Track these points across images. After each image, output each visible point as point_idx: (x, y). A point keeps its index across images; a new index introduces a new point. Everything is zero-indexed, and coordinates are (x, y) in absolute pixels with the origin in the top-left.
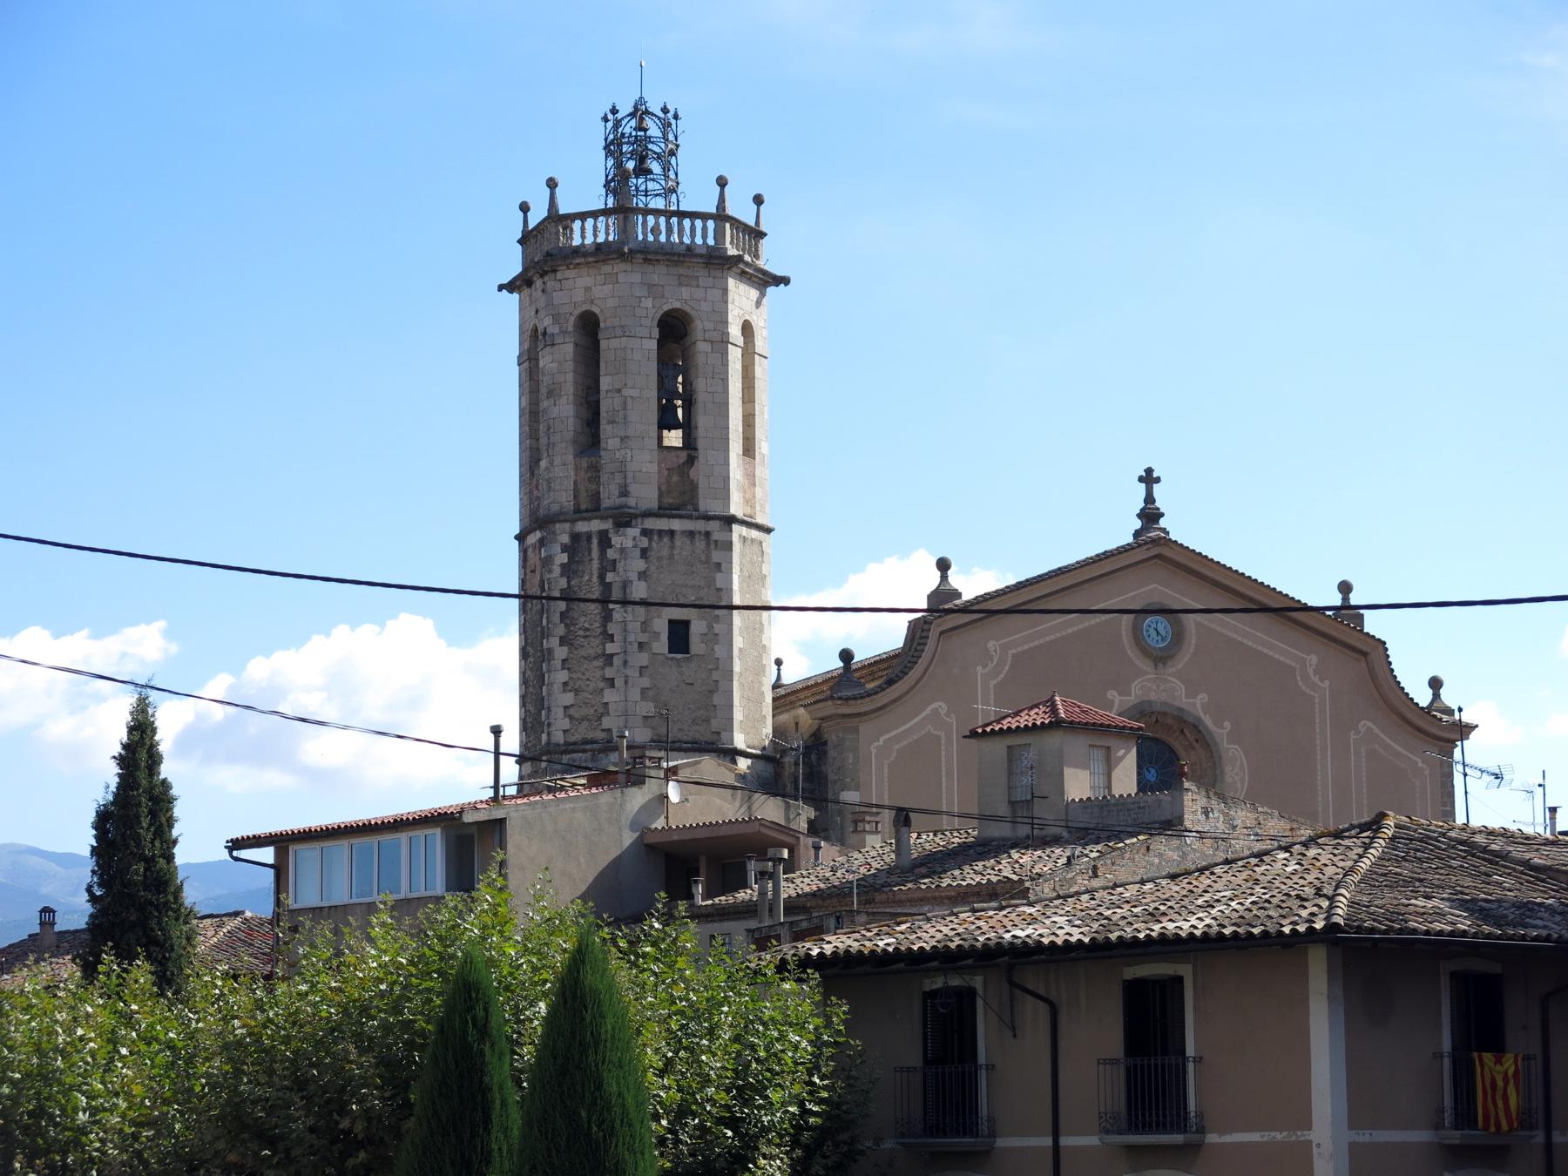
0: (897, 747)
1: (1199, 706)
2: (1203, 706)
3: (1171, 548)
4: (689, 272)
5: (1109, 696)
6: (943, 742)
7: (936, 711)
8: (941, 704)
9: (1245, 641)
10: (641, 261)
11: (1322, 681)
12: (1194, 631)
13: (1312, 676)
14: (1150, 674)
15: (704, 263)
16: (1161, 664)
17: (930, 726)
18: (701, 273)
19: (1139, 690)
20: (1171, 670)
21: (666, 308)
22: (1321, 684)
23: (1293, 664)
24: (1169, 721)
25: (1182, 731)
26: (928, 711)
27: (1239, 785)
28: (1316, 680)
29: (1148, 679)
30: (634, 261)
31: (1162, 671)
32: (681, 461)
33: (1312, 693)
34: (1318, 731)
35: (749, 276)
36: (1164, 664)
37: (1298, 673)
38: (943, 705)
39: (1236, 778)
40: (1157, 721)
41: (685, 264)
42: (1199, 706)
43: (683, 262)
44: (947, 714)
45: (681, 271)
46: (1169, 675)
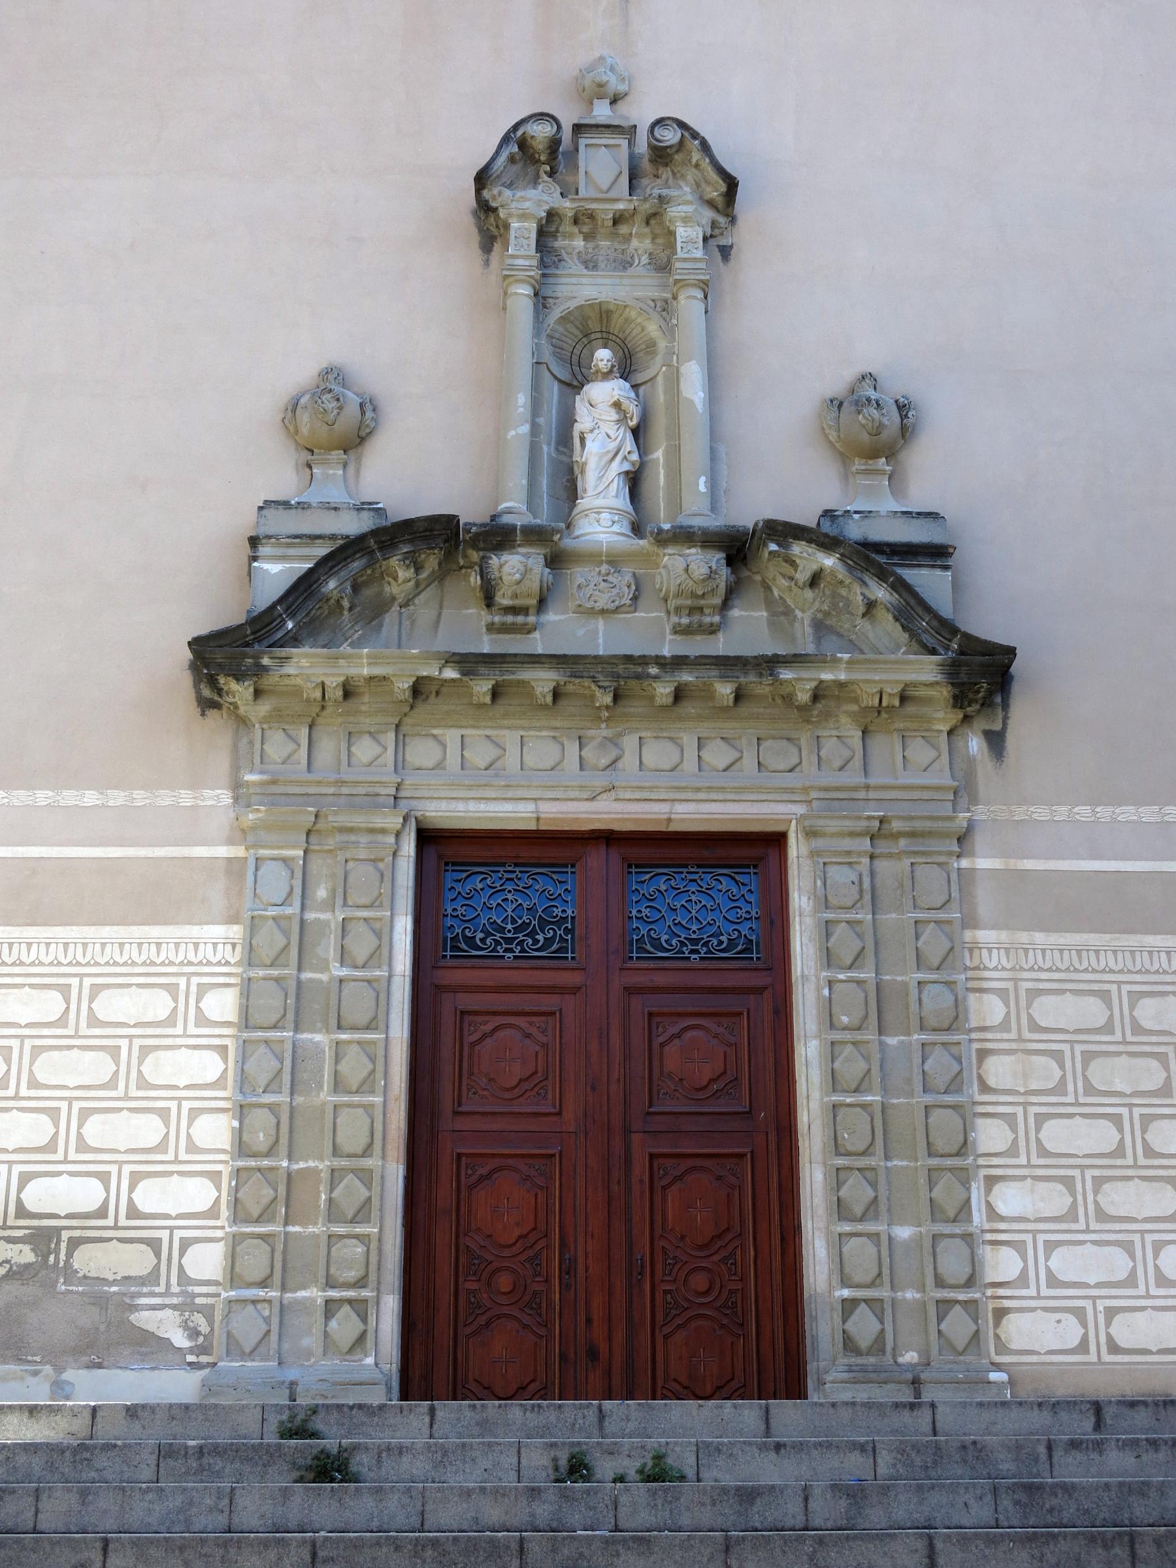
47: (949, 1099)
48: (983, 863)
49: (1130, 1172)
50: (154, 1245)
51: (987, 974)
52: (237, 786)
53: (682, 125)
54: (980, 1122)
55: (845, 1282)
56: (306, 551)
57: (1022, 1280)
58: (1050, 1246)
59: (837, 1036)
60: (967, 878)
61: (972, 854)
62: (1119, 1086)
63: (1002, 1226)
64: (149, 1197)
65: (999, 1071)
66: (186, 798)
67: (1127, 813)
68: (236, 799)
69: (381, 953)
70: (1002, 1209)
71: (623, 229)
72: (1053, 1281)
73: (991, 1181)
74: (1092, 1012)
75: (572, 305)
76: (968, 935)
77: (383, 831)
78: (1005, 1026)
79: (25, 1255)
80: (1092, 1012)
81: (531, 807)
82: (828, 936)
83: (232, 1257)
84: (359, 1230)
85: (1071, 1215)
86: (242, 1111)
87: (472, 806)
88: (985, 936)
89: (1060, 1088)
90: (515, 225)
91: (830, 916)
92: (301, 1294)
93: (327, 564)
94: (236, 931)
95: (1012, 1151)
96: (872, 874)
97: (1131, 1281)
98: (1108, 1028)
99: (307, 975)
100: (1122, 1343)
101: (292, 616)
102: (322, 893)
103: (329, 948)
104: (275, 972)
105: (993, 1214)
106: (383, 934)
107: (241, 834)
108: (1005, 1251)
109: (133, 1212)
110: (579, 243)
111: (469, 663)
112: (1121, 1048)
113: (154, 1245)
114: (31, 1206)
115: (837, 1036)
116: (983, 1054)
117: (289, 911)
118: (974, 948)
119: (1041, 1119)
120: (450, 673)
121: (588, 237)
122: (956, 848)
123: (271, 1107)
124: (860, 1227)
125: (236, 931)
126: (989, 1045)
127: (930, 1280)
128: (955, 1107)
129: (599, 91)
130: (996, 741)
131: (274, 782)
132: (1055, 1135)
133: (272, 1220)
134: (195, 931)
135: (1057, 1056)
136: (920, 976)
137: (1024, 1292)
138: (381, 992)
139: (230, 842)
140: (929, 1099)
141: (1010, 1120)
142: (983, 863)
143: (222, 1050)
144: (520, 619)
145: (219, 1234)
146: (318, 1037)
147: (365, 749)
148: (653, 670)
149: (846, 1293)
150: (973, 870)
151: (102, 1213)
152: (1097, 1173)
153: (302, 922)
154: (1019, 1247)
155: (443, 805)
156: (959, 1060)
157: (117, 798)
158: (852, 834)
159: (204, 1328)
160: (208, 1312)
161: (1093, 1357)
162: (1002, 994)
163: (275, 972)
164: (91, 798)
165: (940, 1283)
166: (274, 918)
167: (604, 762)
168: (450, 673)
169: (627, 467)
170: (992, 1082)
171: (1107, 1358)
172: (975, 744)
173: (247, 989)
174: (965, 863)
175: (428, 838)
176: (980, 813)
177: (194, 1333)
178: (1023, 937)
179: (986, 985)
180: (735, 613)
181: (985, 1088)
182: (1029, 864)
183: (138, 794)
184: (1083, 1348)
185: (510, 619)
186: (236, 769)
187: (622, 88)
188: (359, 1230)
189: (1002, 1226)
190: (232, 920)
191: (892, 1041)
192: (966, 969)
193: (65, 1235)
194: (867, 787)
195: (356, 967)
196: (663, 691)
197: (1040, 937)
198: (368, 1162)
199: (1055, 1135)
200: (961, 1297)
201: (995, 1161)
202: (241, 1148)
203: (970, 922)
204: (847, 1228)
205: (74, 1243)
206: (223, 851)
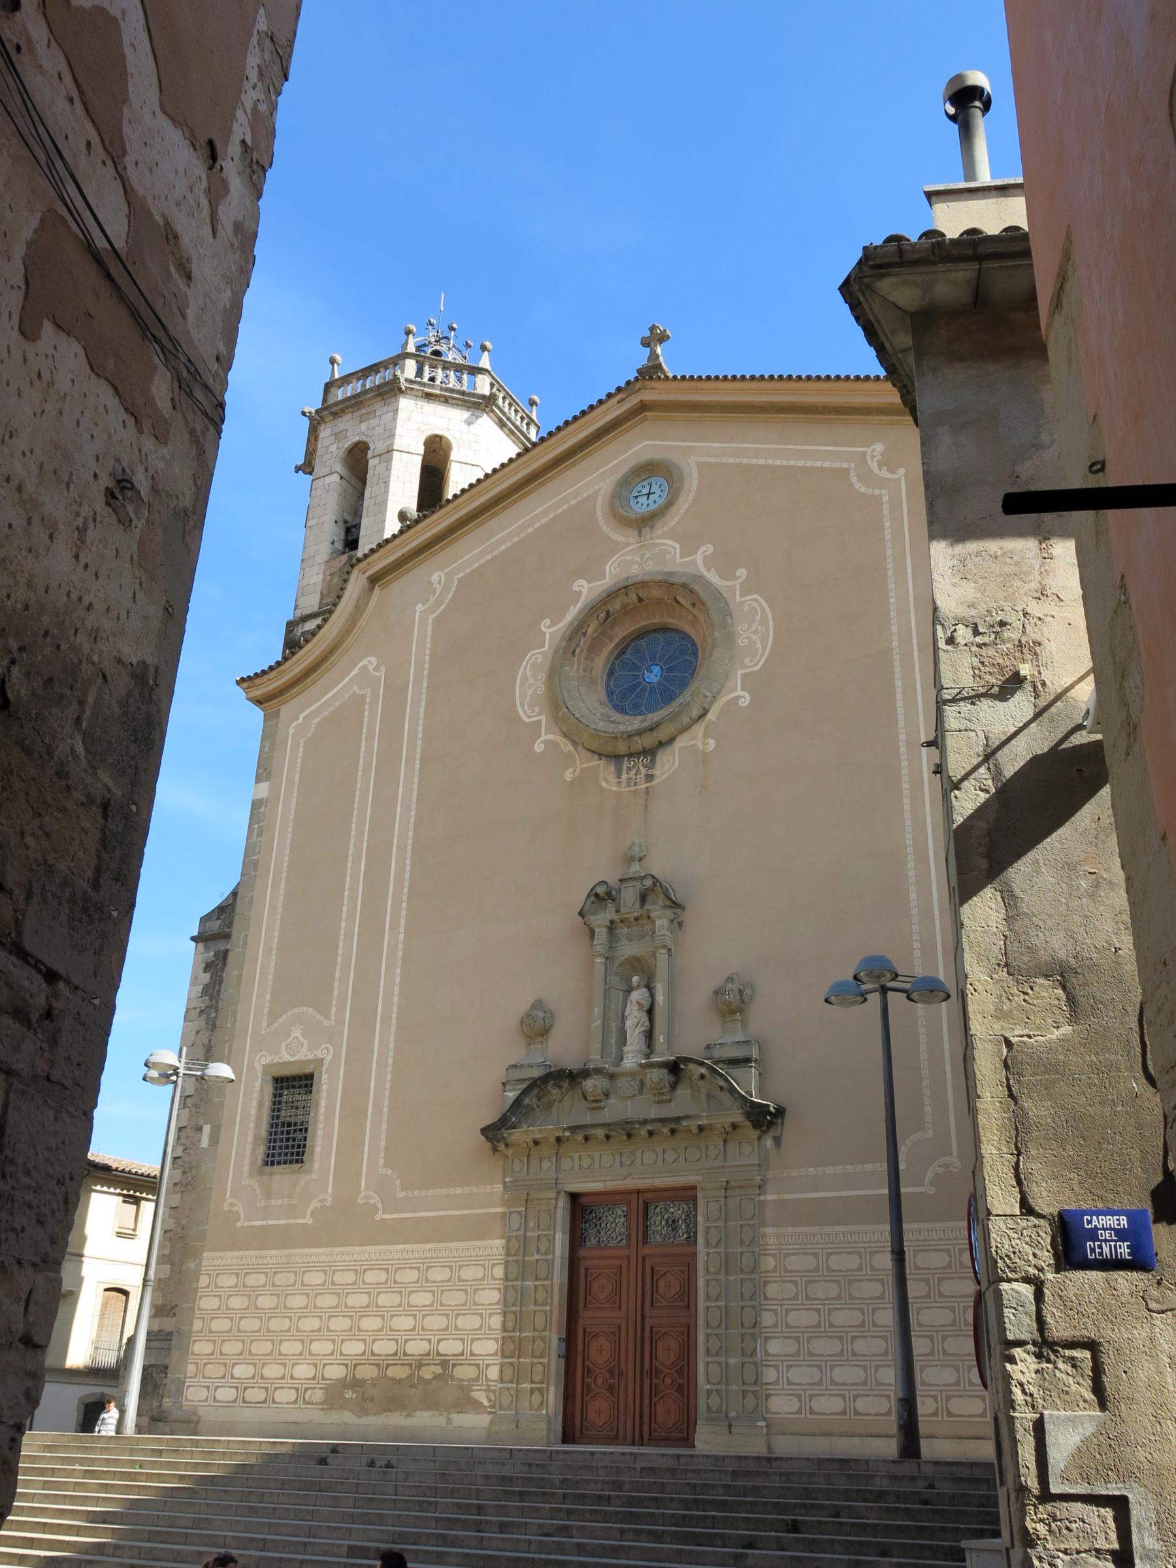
0: (317, 720)
1: (700, 562)
2: (706, 560)
3: (652, 389)
4: (369, 409)
5: (575, 588)
6: (368, 700)
7: (365, 666)
8: (368, 659)
9: (770, 462)
10: (331, 417)
11: (893, 472)
12: (695, 475)
13: (877, 471)
14: (629, 545)
15: (377, 395)
16: (648, 529)
17: (369, 690)
18: (380, 404)
19: (615, 568)
20: (660, 532)
21: (348, 444)
22: (890, 476)
23: (845, 465)
24: (655, 593)
25: (677, 601)
26: (356, 671)
27: (759, 645)
28: (884, 473)
29: (631, 550)
30: (326, 420)
31: (648, 537)
32: (343, 563)
33: (877, 492)
34: (888, 537)
35: (443, 399)
36: (652, 527)
37: (852, 473)
38: (372, 659)
39: (755, 637)
40: (640, 600)
41: (366, 404)
42: (700, 562)
43: (362, 402)
44: (376, 669)
45: (363, 411)
46: (659, 537)
47: (750, 1303)
48: (769, 1197)
49: (822, 1334)
50: (478, 1366)
51: (769, 1247)
52: (504, 1183)
53: (653, 877)
54: (763, 1313)
55: (708, 1382)
56: (517, 1087)
57: (777, 1381)
58: (789, 1367)
59: (709, 1277)
60: (762, 1204)
61: (765, 1194)
62: (820, 1296)
63: (770, 1358)
64: (478, 1348)
65: (772, 1290)
66: (488, 1188)
67: (830, 1170)
68: (504, 1188)
69: (551, 1249)
70: (770, 1351)
71: (640, 922)
72: (789, 1383)
73: (767, 1339)
74: (811, 1262)
75: (622, 959)
76: (762, 1230)
77: (550, 1199)
78: (774, 1271)
79: (439, 1370)
80: (811, 1262)
81: (602, 1184)
82: (708, 1233)
83: (501, 1372)
84: (541, 1360)
85: (798, 1353)
86: (505, 1314)
87: (582, 1185)
88: (769, 1230)
89: (795, 1298)
90: (597, 930)
91: (708, 1225)
92: (524, 1385)
93: (525, 1092)
94: (503, 1242)
95: (775, 1326)
96: (726, 1205)
97: (820, 1383)
98: (816, 1270)
99: (527, 1258)
100: (815, 1410)
101: (514, 1115)
102: (532, 1225)
103: (533, 1248)
104: (515, 1258)
105: (767, 1353)
106: (551, 1241)
107: (504, 1203)
108: (771, 1368)
109: (472, 1354)
110: (626, 930)
111: (574, 1129)
112: (822, 1278)
113: (478, 1366)
114: (441, 1352)
115: (709, 1277)
116: (766, 1283)
117: (520, 1233)
118: (764, 1236)
119: (788, 1311)
120: (567, 1134)
121: (628, 927)
122: (758, 1192)
123: (514, 1313)
124: (714, 1359)
125: (503, 1242)
126: (768, 1279)
127: (741, 1383)
128: (753, 1307)
129: (630, 859)
130: (777, 1140)
131: (515, 1181)
132: (793, 1318)
133: (513, 1357)
134: (490, 1242)
135: (795, 1283)
136: (741, 1249)
137: (778, 1387)
138: (550, 1264)
139: (502, 1206)
140: (742, 1303)
141: (775, 1311)
142: (769, 1197)
143: (499, 1289)
144: (598, 1105)
145: (498, 1362)
146: (530, 1283)
147: (546, 1164)
148: (637, 1126)
149: (708, 1387)
150: (765, 1201)
151: (462, 1354)
152: (809, 1335)
153: (525, 1236)
154: (776, 1367)
155: (573, 1186)
156: (755, 1286)
157: (467, 1190)
158: (717, 1189)
159: (493, 1399)
160: (494, 1392)
161: (803, 1416)
162: (774, 1256)
163: (515, 1258)
164: (459, 1191)
165: (744, 1383)
166: (516, 1236)
167: (628, 1163)
168: (567, 1134)
169: (643, 1029)
170: (769, 1295)
171: (809, 1416)
172: (769, 1143)
173: (507, 1265)
174: (762, 1198)
175: (574, 1197)
176: (770, 1174)
177: (490, 1400)
178: (783, 1230)
179: (767, 1252)
180: (678, 1092)
181: (766, 1298)
182: (788, 1196)
183: (474, 1188)
184: (799, 1411)
185: (594, 1105)
186: (504, 1176)
187: (642, 855)
188: (541, 1360)
189: (770, 1358)
190: (503, 1237)
191: (731, 1278)
192: (760, 1245)
193: (451, 1362)
194: (724, 1167)
195: (542, 1255)
196: (643, 1132)
197: (790, 1230)
198: (546, 1334)
199: (793, 1318)
200: (752, 1389)
201: (770, 1330)
202: (504, 1329)
203: (763, 1224)
204: (710, 1359)
205: (454, 1365)
206: (500, 1210)
